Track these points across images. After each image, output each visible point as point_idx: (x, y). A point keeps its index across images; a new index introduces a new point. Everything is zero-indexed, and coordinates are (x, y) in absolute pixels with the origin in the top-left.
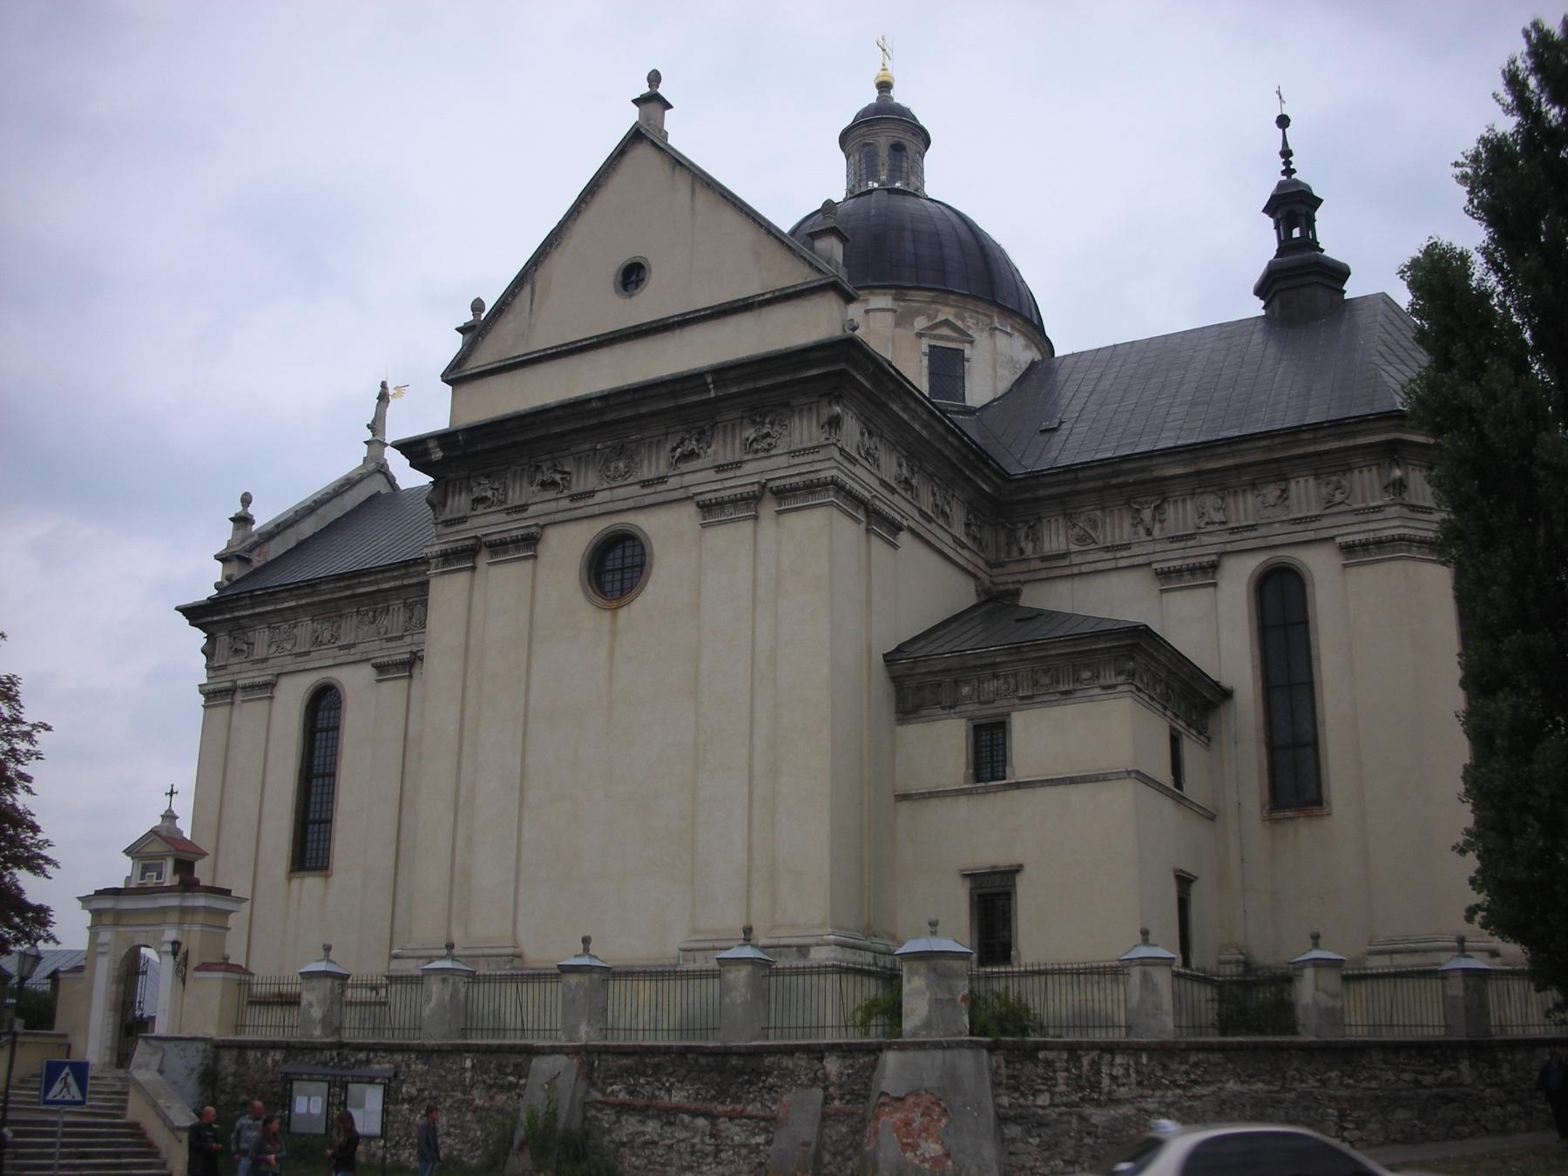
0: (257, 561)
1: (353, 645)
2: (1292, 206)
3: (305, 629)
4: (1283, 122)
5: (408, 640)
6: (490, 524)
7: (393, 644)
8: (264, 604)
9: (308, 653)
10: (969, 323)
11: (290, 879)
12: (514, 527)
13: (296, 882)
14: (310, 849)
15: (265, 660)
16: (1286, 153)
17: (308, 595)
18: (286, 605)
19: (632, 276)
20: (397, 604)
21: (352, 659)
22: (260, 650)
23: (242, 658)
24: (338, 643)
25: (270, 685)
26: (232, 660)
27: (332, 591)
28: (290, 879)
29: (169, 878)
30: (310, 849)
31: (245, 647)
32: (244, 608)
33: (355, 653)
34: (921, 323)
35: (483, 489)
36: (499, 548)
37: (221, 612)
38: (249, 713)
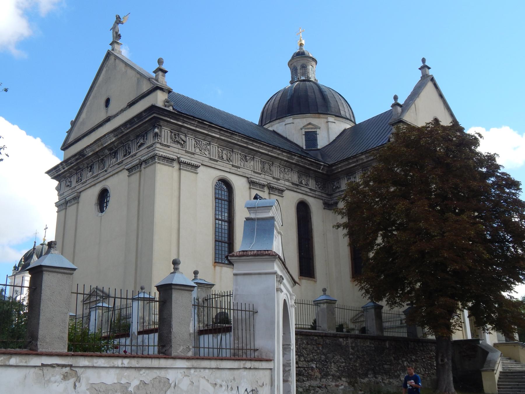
1: (239, 168)
3: (214, 149)
5: (263, 176)
7: (257, 175)
8: (204, 128)
9: (217, 161)
11: (215, 266)
13: (218, 268)
15: (193, 154)
17: (226, 136)
18: (214, 135)
20: (257, 158)
21: (238, 173)
23: (179, 146)
24: (231, 163)
25: (197, 167)
26: (174, 145)
27: (238, 141)
28: (215, 266)
31: (182, 142)
32: (191, 124)
33: (241, 171)
37: (177, 120)
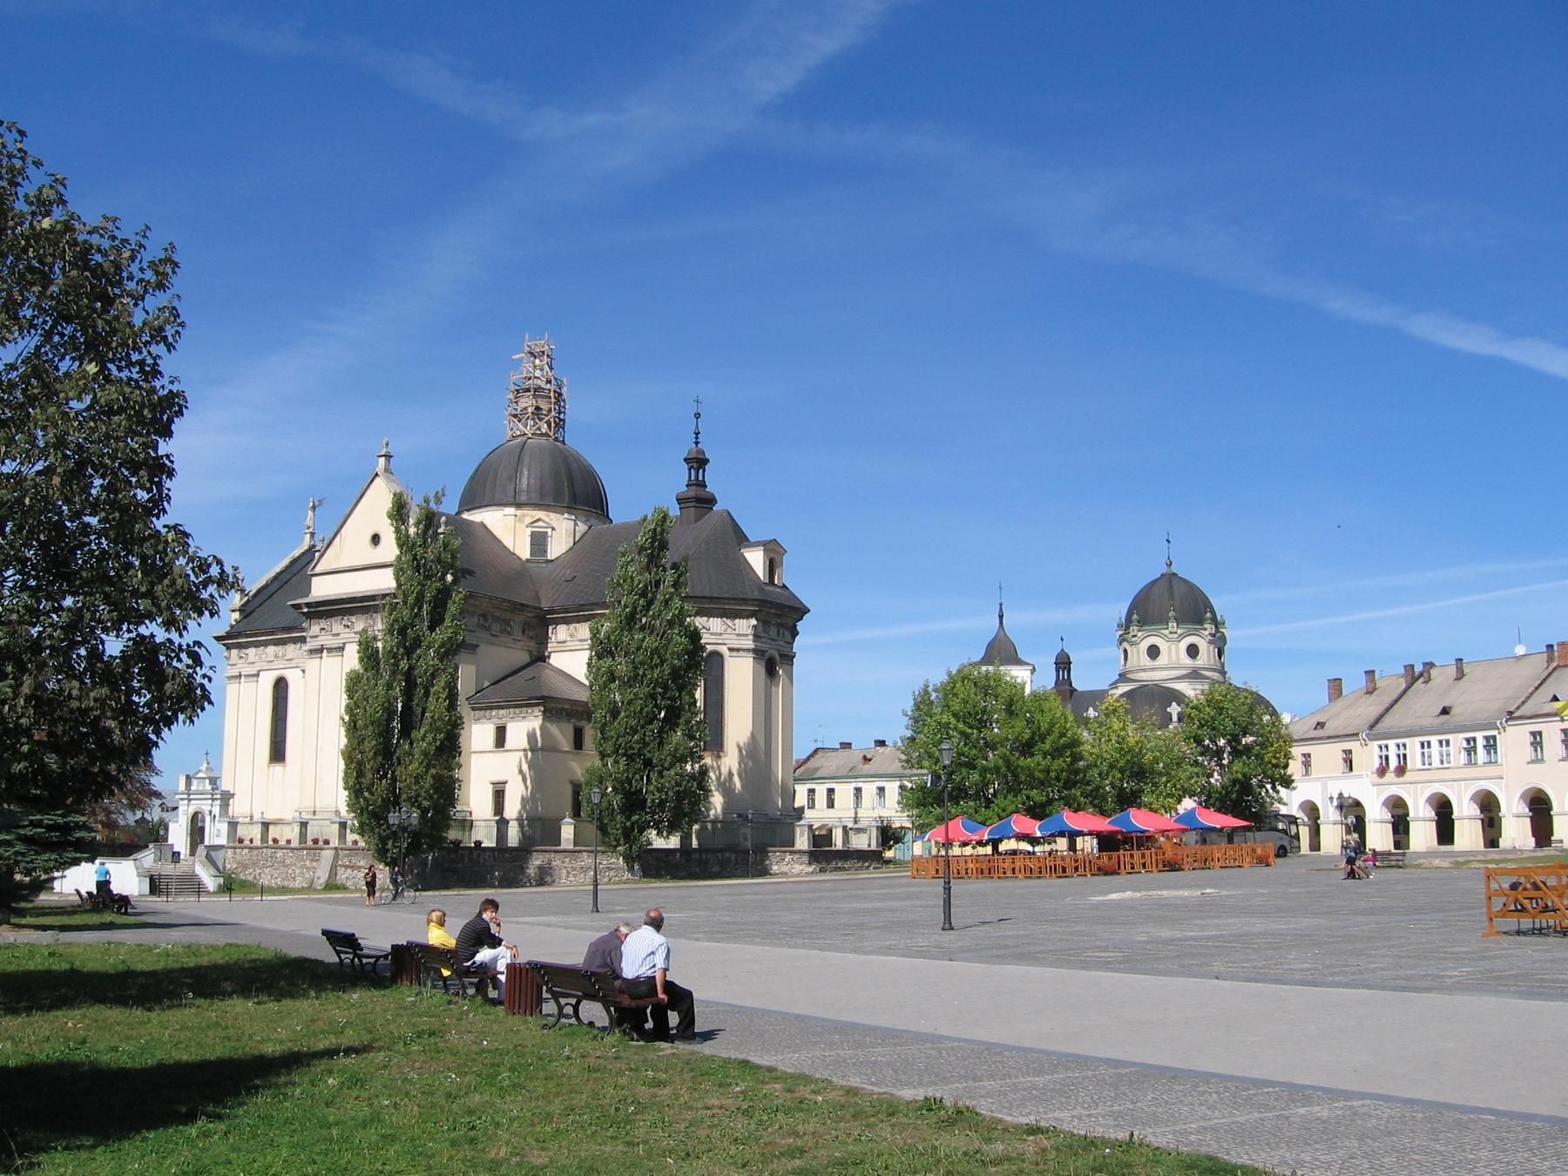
0: (249, 609)
2: (698, 462)
3: (271, 649)
4: (697, 416)
6: (327, 640)
10: (553, 515)
12: (335, 642)
14: (278, 753)
16: (697, 434)
19: (376, 539)
22: (252, 658)
29: (209, 787)
30: (278, 753)
34: (528, 520)
35: (323, 623)
36: (330, 650)
38: (246, 686)
